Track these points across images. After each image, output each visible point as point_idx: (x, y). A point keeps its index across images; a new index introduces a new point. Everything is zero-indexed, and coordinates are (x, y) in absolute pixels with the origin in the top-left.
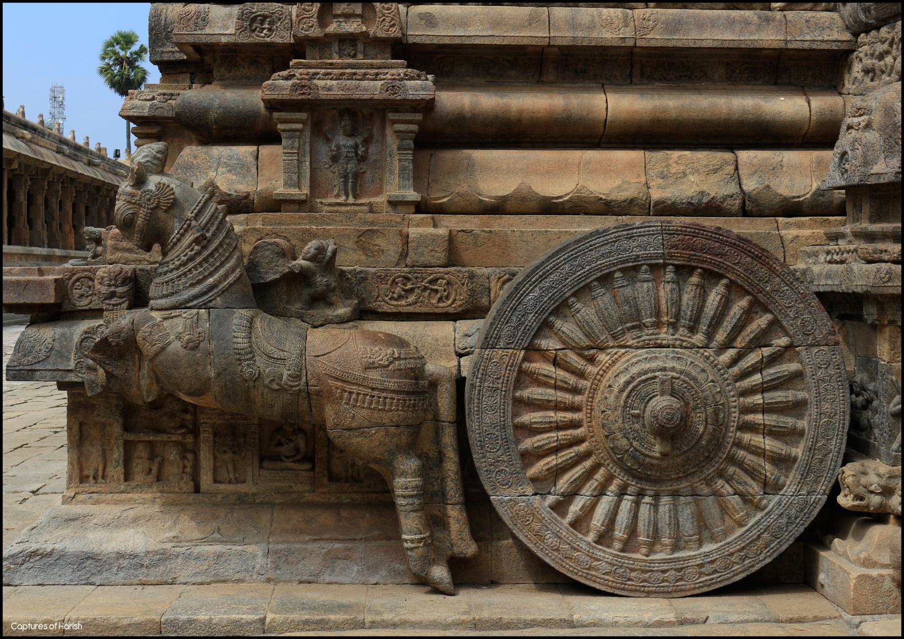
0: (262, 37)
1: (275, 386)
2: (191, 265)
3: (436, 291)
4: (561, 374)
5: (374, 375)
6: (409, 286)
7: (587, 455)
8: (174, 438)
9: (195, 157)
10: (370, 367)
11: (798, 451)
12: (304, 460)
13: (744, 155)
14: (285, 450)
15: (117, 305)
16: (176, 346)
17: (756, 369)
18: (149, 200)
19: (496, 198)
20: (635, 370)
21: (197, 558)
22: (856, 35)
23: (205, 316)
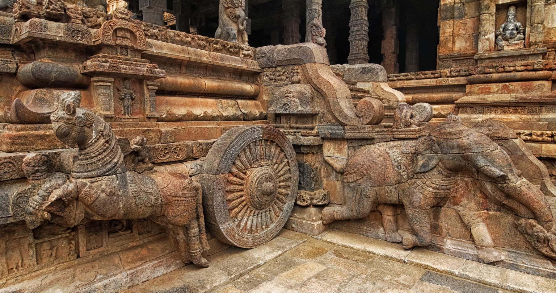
0: (79, 40)
1: (149, 205)
2: (105, 154)
3: (176, 153)
4: (238, 180)
5: (185, 192)
6: (166, 152)
7: (245, 205)
8: (65, 235)
9: (45, 95)
10: (184, 189)
11: (289, 192)
12: (126, 229)
13: (239, 101)
14: (118, 227)
15: (40, 176)
16: (103, 195)
17: (281, 169)
18: (80, 122)
19: (181, 115)
20: (258, 175)
21: (95, 290)
22: (263, 68)
23: (116, 179)
